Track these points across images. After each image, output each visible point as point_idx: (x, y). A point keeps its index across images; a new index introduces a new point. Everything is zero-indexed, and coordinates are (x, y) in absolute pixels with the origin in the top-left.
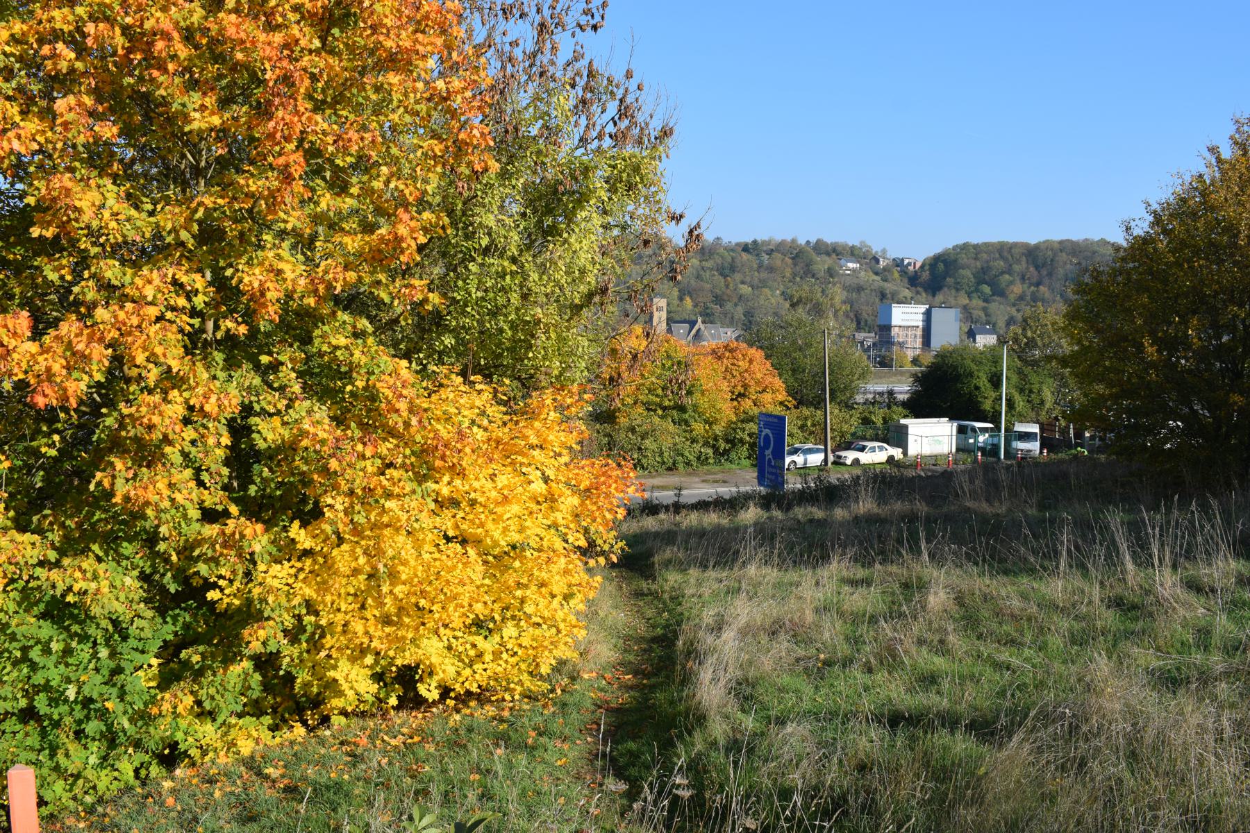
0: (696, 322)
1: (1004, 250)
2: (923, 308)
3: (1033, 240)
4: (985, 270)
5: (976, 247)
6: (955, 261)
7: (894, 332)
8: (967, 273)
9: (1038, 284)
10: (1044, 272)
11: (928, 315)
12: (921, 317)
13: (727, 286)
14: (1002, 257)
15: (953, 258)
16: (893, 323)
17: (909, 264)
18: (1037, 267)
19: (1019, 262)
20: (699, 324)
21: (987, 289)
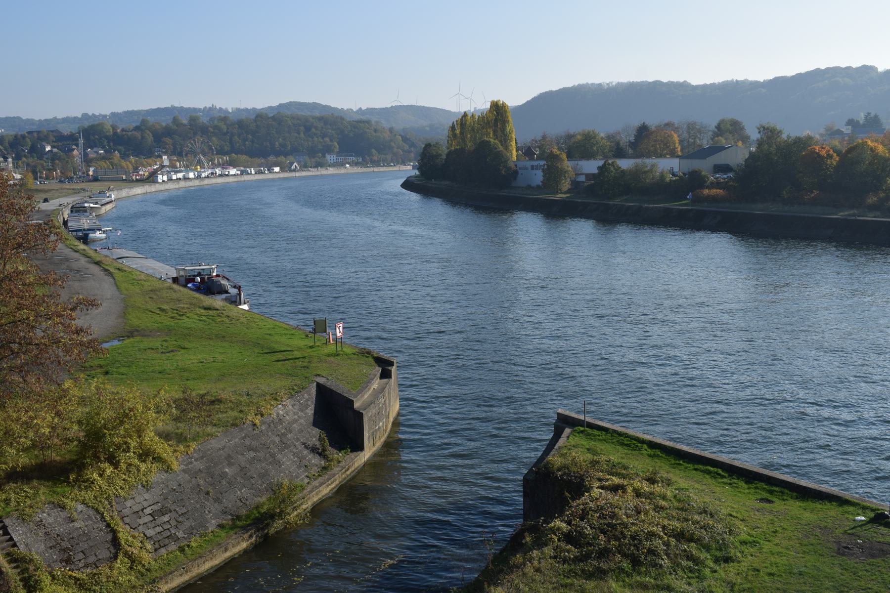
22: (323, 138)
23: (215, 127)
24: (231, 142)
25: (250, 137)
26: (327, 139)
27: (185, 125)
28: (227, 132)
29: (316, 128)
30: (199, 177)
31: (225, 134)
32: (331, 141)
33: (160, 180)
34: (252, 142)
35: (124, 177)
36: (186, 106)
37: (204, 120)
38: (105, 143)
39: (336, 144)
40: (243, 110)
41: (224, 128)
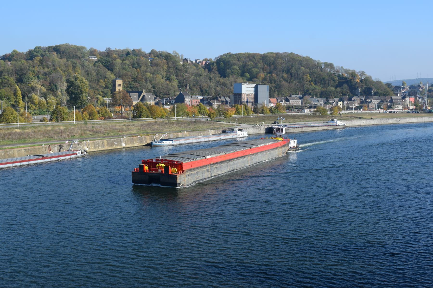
0: (142, 92)
1: (251, 57)
2: (253, 85)
3: (262, 52)
4: (244, 66)
5: (235, 55)
6: (229, 61)
7: (243, 96)
8: (236, 67)
9: (271, 73)
10: (272, 67)
11: (256, 88)
12: (253, 89)
13: (138, 73)
14: (250, 60)
15: (227, 60)
16: (243, 92)
17: (199, 62)
18: (267, 65)
19: (259, 62)
20: (144, 93)
21: (248, 75)
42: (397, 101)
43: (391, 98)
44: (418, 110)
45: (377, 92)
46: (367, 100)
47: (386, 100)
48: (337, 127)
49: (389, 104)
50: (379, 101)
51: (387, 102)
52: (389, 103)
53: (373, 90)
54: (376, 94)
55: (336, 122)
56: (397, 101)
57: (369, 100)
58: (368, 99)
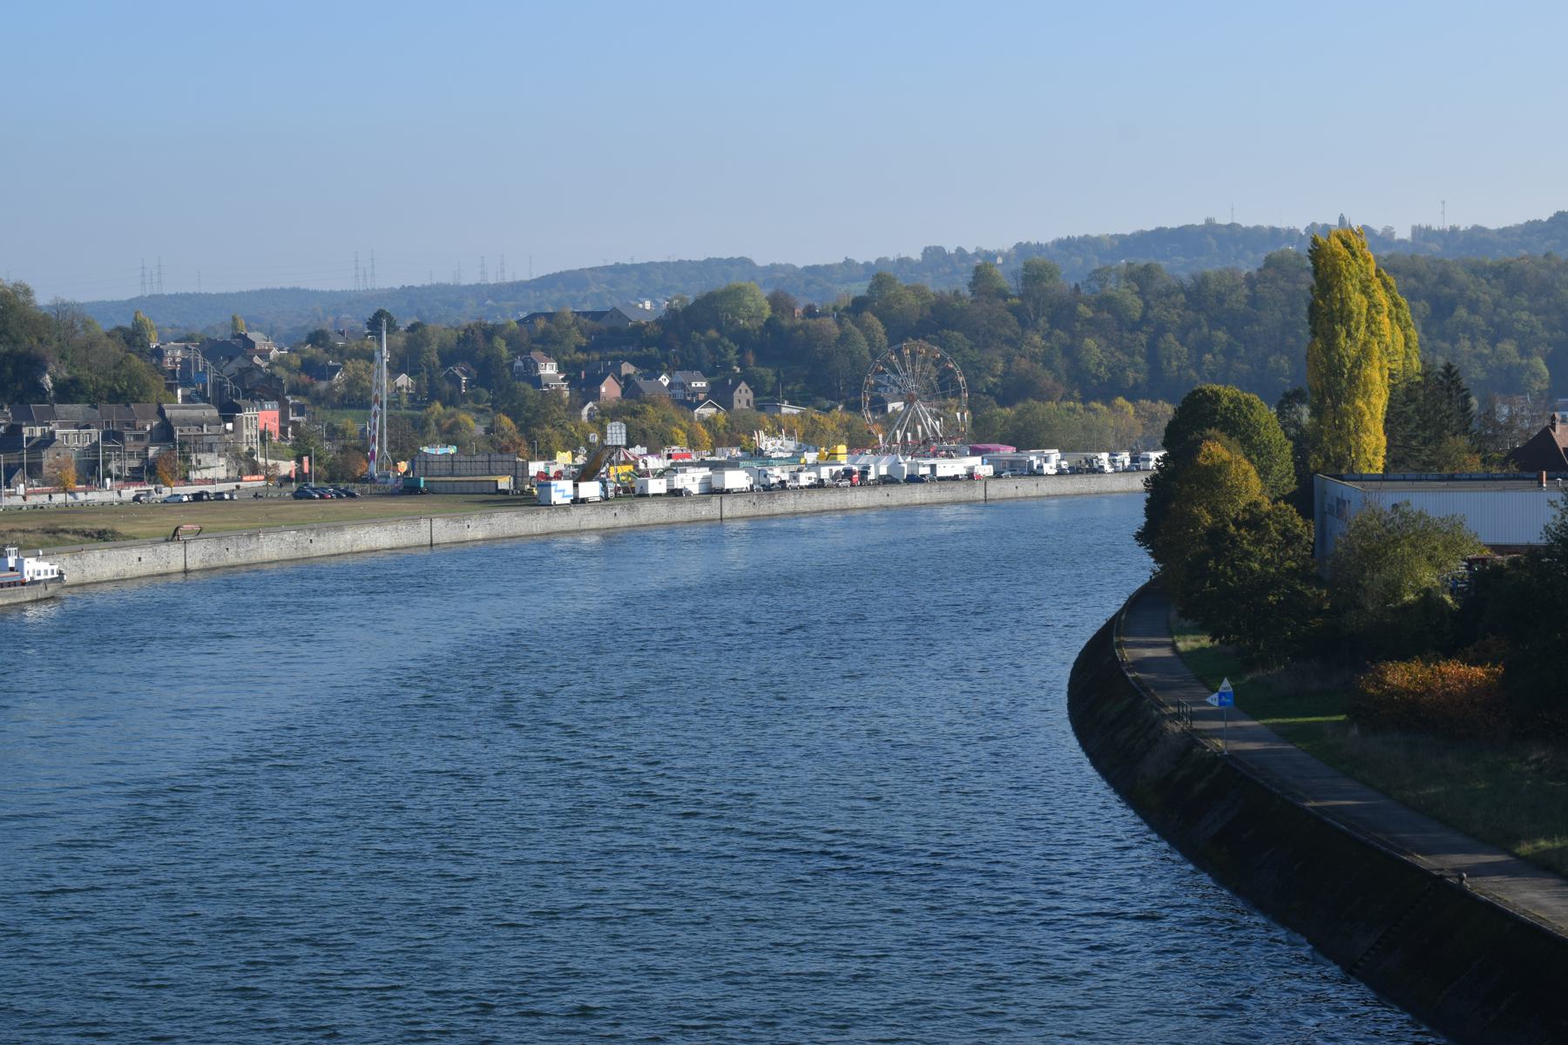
22: (1493, 342)
23: (1105, 303)
24: (1153, 356)
25: (1221, 335)
26: (1508, 347)
27: (1003, 294)
28: (1144, 319)
29: (1473, 307)
30: (712, 491)
31: (1135, 327)
32: (1524, 352)
33: (556, 498)
34: (1230, 352)
35: (504, 483)
36: (1247, 221)
37: (1068, 277)
38: (732, 355)
39: (1540, 364)
40: (1441, 234)
41: (1134, 304)
42: (194, 430)
43: (161, 412)
44: (334, 480)
45: (74, 381)
46: (26, 431)
47: (132, 425)
48: (27, 595)
49: (152, 451)
50: (96, 433)
51: (138, 438)
52: (154, 442)
53: (52, 368)
54: (68, 391)
55: (20, 562)
56: (194, 430)
57: (38, 432)
58: (32, 422)
